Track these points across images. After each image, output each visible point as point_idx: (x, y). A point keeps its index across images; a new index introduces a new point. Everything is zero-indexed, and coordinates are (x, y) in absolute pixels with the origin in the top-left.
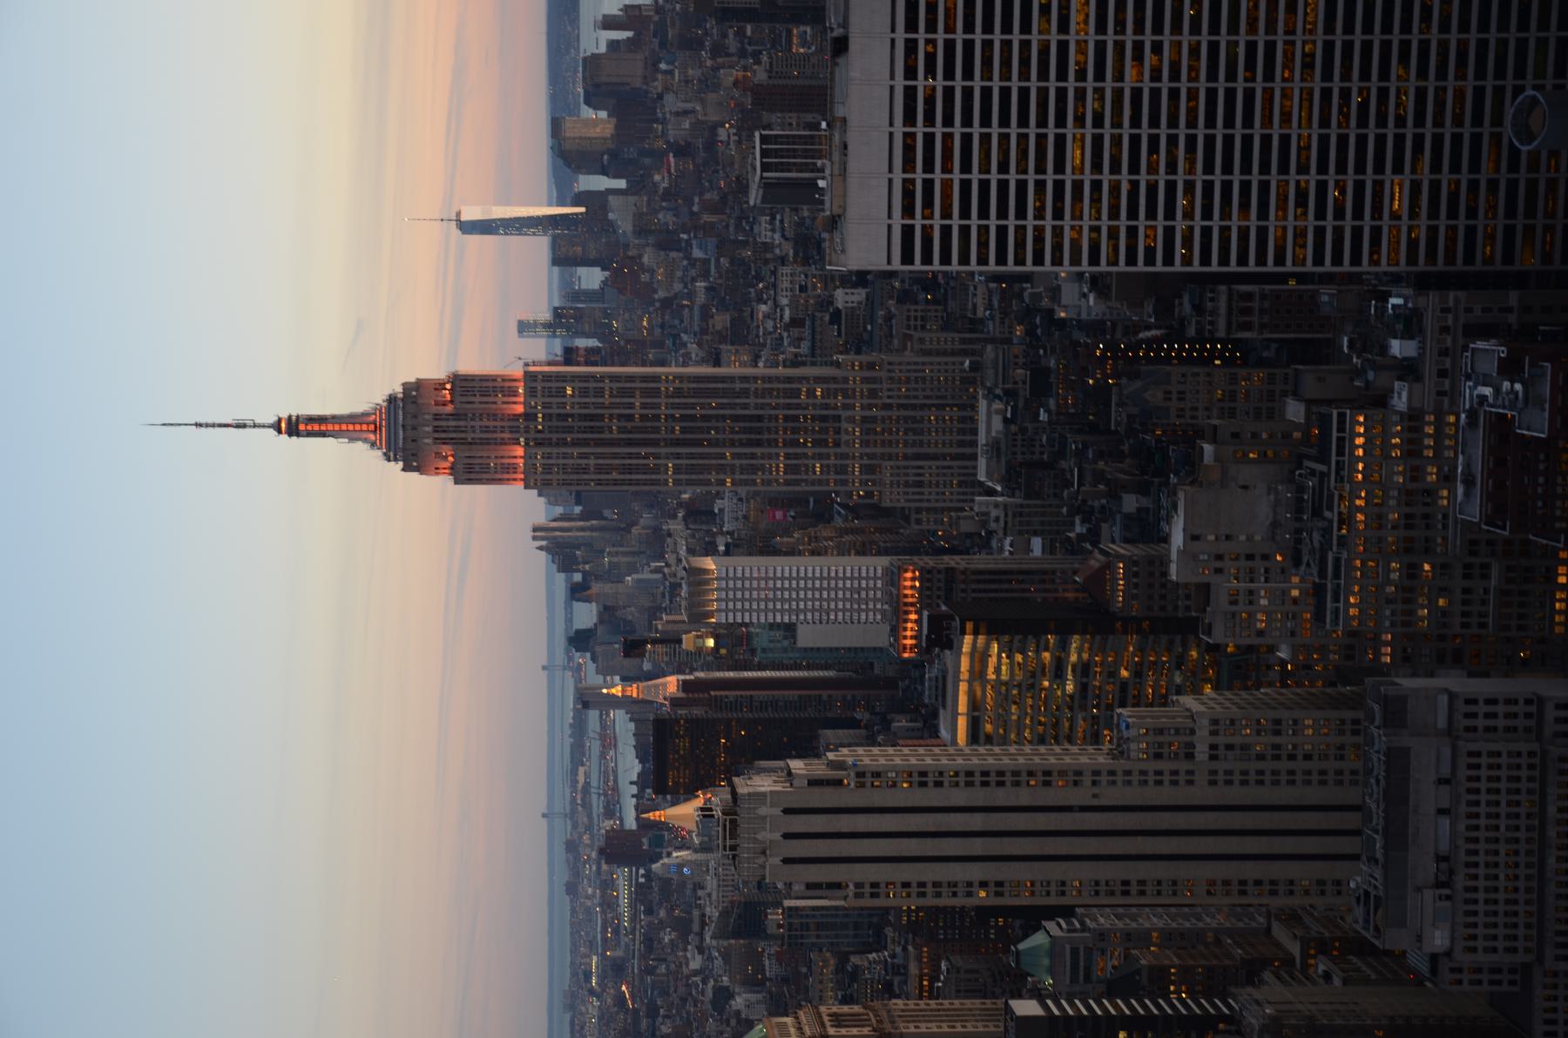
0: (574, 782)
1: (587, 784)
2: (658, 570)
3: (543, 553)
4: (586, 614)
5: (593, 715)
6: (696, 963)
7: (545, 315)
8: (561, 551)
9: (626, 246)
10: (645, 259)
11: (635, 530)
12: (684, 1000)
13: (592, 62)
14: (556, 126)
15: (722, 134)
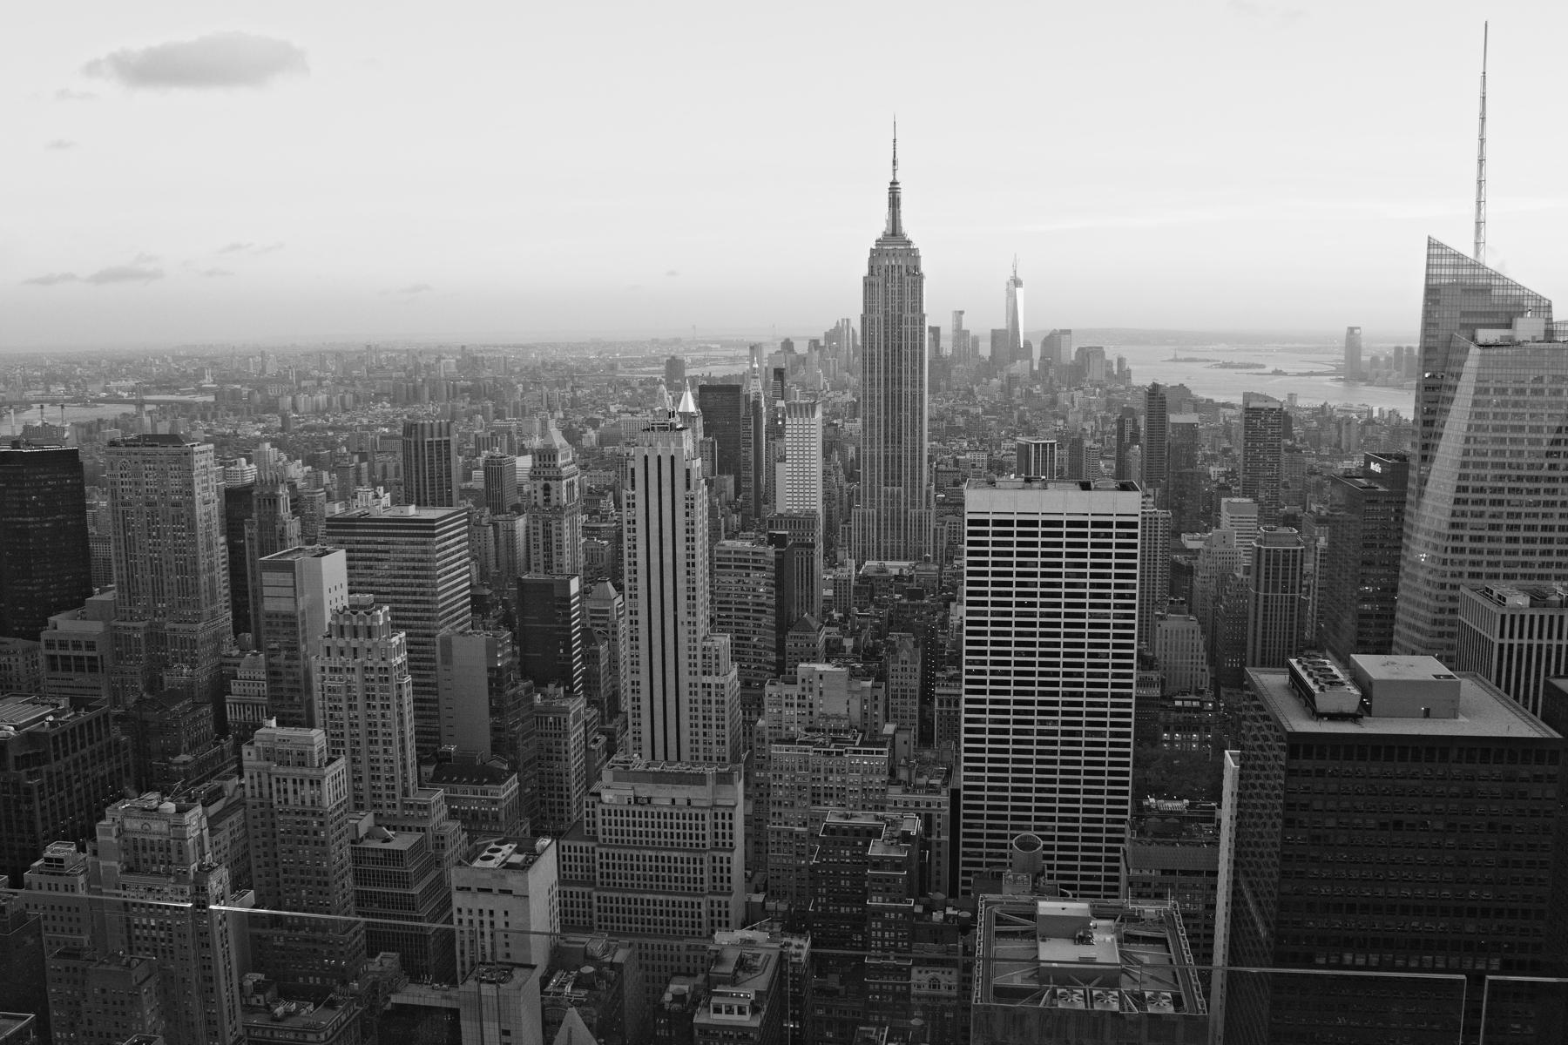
0: (712, 342)
1: (710, 349)
2: (825, 387)
3: (833, 326)
4: (801, 348)
5: (747, 352)
6: (613, 409)
7: (964, 327)
8: (834, 335)
9: (1002, 370)
10: (995, 380)
11: (847, 374)
12: (594, 403)
13: (1099, 351)
14: (1068, 332)
15: (1060, 422)
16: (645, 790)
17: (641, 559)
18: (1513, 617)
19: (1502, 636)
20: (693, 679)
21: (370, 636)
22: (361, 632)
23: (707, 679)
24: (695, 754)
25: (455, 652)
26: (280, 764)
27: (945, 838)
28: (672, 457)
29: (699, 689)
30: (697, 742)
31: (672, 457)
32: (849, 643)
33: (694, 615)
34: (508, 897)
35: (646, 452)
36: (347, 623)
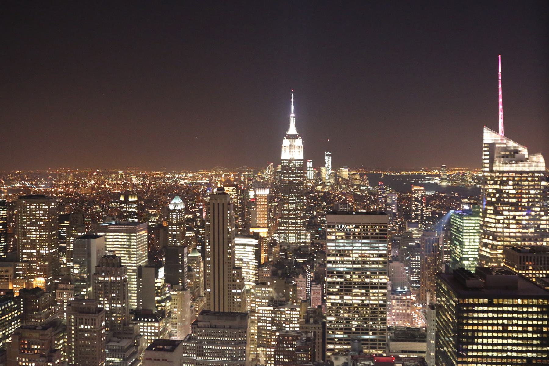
16: (215, 322)
17: (212, 240)
18: (524, 257)
19: (520, 264)
20: (229, 283)
21: (114, 267)
22: (111, 265)
23: (234, 283)
24: (229, 310)
25: (143, 273)
26: (81, 312)
27: (321, 340)
28: (223, 204)
29: (232, 287)
30: (230, 306)
31: (223, 204)
32: (280, 272)
33: (230, 260)
34: (166, 362)
35: (214, 202)
36: (106, 262)
